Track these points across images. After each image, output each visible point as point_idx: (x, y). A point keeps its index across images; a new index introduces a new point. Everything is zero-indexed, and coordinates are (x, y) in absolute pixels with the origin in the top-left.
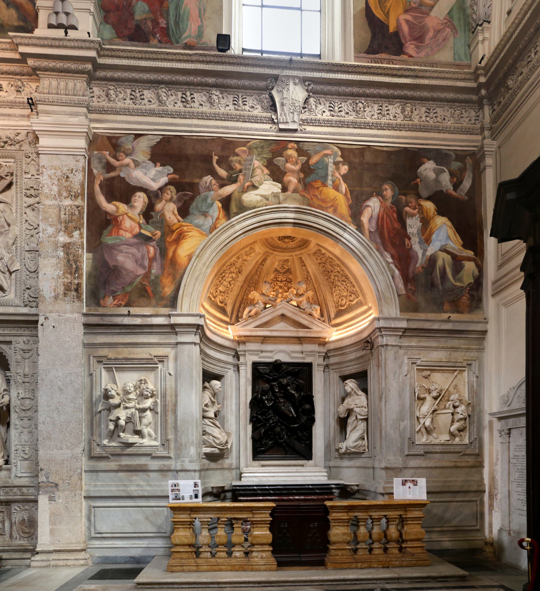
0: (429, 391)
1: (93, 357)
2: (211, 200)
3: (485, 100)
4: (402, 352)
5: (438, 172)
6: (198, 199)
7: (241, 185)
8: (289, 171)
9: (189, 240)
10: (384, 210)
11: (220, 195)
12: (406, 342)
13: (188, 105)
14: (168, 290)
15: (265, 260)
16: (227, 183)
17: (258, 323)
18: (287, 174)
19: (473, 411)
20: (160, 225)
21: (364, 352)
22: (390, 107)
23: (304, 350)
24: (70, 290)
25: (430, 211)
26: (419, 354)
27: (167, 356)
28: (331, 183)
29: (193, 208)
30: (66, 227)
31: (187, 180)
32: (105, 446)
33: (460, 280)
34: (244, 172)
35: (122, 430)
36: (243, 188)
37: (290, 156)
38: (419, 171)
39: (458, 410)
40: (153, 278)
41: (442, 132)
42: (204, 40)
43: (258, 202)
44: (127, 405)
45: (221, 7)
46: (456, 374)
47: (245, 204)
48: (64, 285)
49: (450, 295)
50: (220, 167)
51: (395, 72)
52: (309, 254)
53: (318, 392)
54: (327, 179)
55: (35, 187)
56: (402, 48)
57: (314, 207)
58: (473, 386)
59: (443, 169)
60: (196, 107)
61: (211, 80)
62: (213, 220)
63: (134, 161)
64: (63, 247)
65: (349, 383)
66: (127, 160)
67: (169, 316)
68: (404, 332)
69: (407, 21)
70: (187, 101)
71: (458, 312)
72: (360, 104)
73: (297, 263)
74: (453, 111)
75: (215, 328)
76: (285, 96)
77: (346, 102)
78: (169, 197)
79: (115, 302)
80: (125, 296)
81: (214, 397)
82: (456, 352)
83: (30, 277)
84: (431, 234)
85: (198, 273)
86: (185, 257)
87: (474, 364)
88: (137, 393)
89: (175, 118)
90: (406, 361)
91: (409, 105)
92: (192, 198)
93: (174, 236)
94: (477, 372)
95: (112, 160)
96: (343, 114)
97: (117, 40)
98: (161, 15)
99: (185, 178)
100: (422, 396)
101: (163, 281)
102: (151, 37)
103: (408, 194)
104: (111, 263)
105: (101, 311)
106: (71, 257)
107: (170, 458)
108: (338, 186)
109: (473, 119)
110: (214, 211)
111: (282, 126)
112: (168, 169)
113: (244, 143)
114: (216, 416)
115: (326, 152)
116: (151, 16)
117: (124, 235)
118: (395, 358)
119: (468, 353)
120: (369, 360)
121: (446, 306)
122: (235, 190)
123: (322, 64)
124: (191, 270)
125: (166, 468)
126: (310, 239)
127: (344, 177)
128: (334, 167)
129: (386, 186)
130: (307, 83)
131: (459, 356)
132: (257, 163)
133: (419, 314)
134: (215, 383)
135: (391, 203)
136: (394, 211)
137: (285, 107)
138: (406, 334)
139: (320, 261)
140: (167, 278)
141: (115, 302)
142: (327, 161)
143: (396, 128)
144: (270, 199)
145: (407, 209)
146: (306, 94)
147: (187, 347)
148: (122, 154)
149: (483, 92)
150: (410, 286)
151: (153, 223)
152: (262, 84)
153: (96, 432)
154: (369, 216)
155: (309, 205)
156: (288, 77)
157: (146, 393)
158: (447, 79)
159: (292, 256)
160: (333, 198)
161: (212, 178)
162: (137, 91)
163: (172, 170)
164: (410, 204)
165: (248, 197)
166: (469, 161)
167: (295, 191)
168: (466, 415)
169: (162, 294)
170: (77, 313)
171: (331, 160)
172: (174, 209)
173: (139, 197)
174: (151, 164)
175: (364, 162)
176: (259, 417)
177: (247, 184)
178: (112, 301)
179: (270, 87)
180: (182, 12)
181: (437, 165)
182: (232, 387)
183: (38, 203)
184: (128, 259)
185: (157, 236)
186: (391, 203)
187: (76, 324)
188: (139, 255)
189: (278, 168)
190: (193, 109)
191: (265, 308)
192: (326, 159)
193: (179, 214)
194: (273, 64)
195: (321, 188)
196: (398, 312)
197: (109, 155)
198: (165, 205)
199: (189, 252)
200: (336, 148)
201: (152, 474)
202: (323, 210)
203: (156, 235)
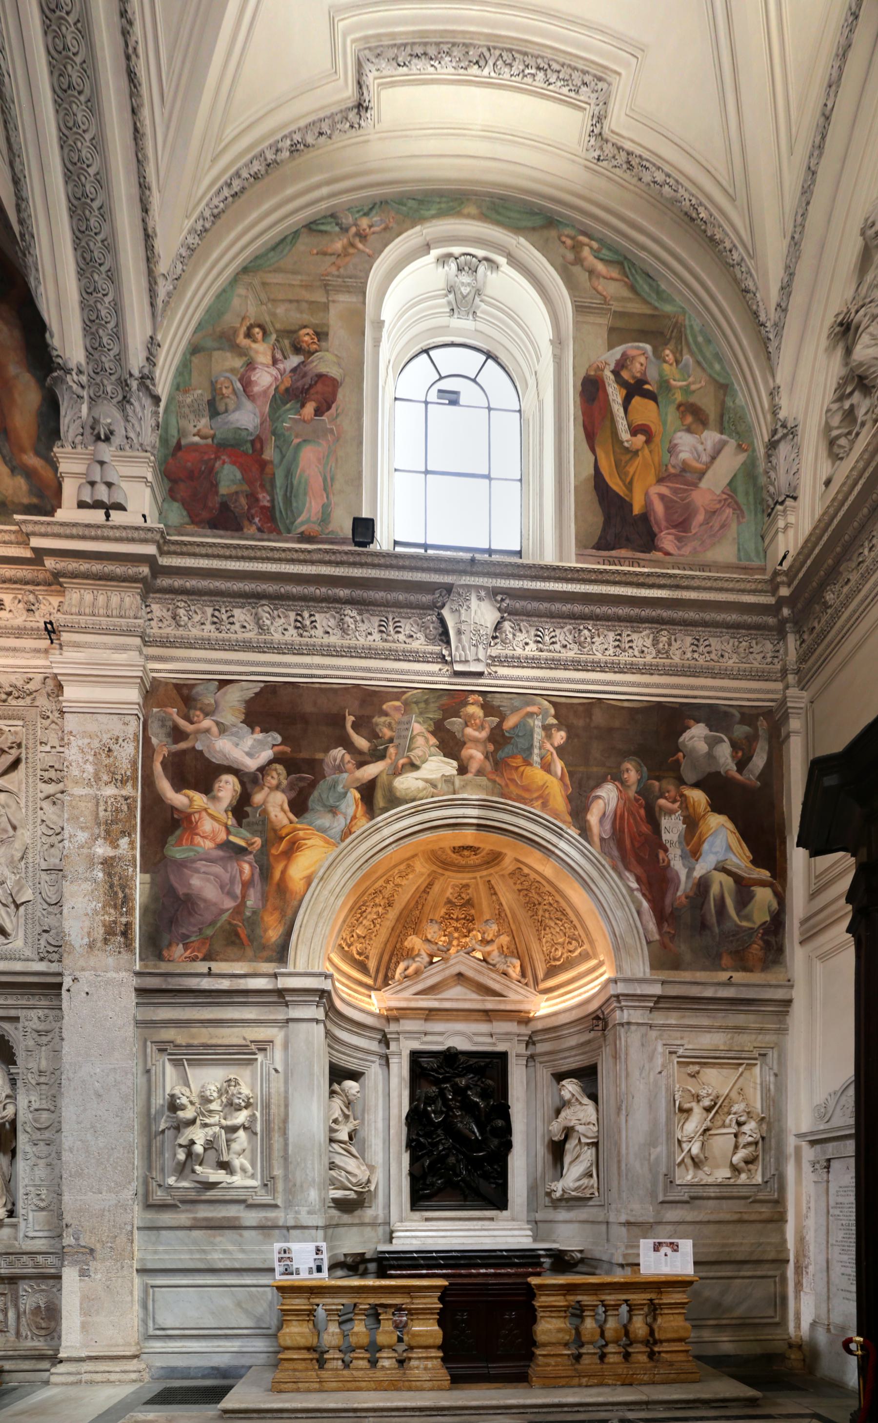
0: (698, 1098)
3: (788, 625)
4: (653, 1034)
5: (713, 743)
6: (322, 786)
9: (307, 852)
11: (358, 779)
12: (659, 1018)
13: (305, 634)
14: (273, 934)
15: (430, 885)
16: (369, 759)
17: (420, 987)
19: (769, 1130)
21: (592, 1034)
22: (634, 636)
23: (494, 1031)
24: (114, 934)
25: (699, 805)
26: (682, 1038)
28: (538, 760)
30: (108, 832)
31: (304, 755)
32: (170, 1187)
33: (748, 918)
34: (396, 741)
36: (396, 767)
37: (472, 716)
38: (681, 740)
39: (746, 1128)
42: (331, 527)
43: (419, 790)
44: (207, 1121)
45: (360, 473)
46: (741, 1070)
47: (398, 794)
48: (104, 925)
49: (732, 942)
51: (642, 580)
52: (503, 875)
53: (518, 1099)
54: (531, 754)
55: (56, 767)
56: (653, 541)
57: (510, 799)
60: (318, 637)
61: (343, 593)
63: (218, 723)
64: (102, 863)
66: (207, 723)
67: (275, 976)
68: (656, 1003)
69: (662, 497)
70: (304, 627)
71: (745, 969)
72: (586, 632)
73: (483, 889)
74: (736, 643)
75: (350, 995)
76: (463, 619)
77: (562, 628)
78: (274, 782)
79: (187, 954)
80: (204, 943)
81: (348, 1108)
83: (49, 913)
85: (322, 905)
87: (770, 1053)
89: (284, 653)
90: (660, 1049)
91: (664, 633)
92: (313, 785)
93: (283, 845)
94: (775, 1067)
95: (182, 723)
96: (557, 647)
97: (190, 528)
98: (262, 486)
100: (686, 1106)
101: (266, 919)
102: (246, 523)
103: (664, 777)
104: (181, 891)
105: (164, 967)
106: (116, 880)
107: (276, 1206)
108: (550, 765)
109: (769, 655)
110: (348, 806)
111: (458, 667)
114: (351, 1138)
115: (530, 709)
116: (245, 487)
118: (643, 1045)
119: (760, 1037)
120: (600, 1047)
121: (726, 960)
122: (382, 772)
123: (523, 566)
125: (269, 1224)
126: (504, 851)
127: (560, 750)
128: (543, 734)
129: (628, 765)
130: (499, 598)
131: (747, 1041)
132: (417, 727)
134: (350, 1085)
136: (641, 806)
137: (463, 636)
139: (520, 887)
140: (272, 914)
141: (187, 954)
144: (439, 786)
145: (662, 801)
146: (498, 615)
147: (304, 1026)
148: (198, 713)
149: (786, 612)
150: (666, 928)
151: (249, 824)
152: (426, 598)
153: (157, 1165)
154: (600, 814)
155: (503, 795)
156: (468, 587)
157: (237, 1101)
158: (727, 590)
159: (475, 878)
160: (541, 783)
162: (223, 610)
163: (279, 739)
166: (762, 724)
167: (480, 773)
168: (757, 1136)
169: (263, 941)
170: (126, 970)
171: (538, 723)
174: (245, 728)
175: (593, 725)
176: (422, 1140)
177: (401, 762)
179: (439, 604)
180: (295, 482)
181: (711, 730)
182: (377, 1092)
183: (62, 792)
184: (208, 884)
187: (123, 989)
188: (226, 877)
189: (452, 734)
190: (314, 639)
191: (431, 963)
192: (530, 721)
193: (292, 810)
194: (443, 566)
195: (522, 769)
196: (648, 970)
197: (178, 714)
198: (268, 795)
199: (307, 873)
200: (546, 703)
201: (247, 1234)
202: (525, 804)
203: (253, 844)
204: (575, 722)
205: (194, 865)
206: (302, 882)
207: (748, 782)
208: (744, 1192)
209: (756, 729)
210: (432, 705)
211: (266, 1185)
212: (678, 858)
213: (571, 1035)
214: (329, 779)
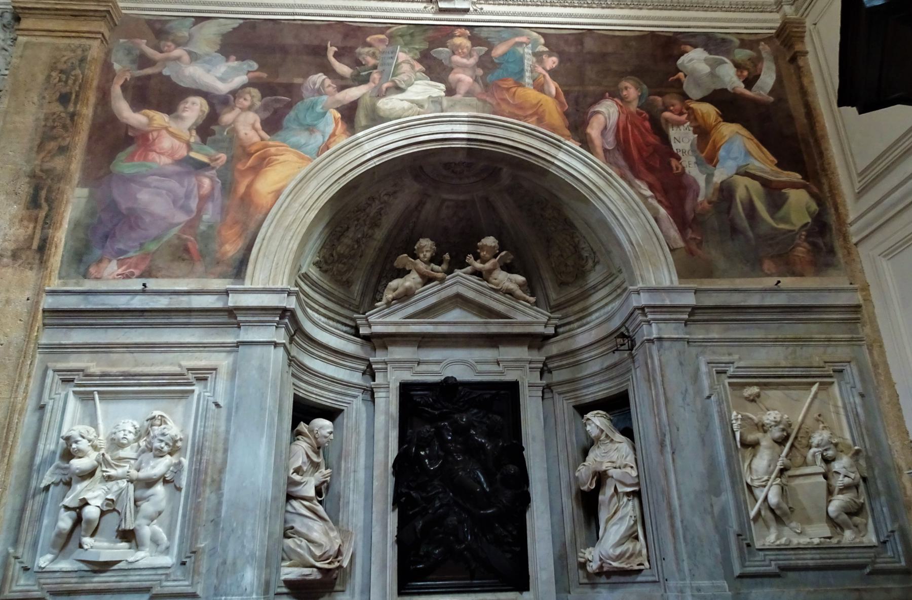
0: (762, 428)
1: (55, 371)
2: (322, 108)
4: (694, 350)
5: (714, 65)
6: (300, 106)
8: (458, 66)
9: (278, 168)
10: (627, 117)
11: (338, 101)
12: (698, 333)
14: (231, 249)
17: (411, 310)
18: (455, 71)
19: (870, 467)
23: (500, 358)
25: (709, 115)
27: (215, 369)
28: (531, 81)
31: (282, 79)
32: (42, 571)
34: (380, 68)
35: (91, 532)
36: (380, 90)
37: (459, 46)
38: (679, 62)
39: (837, 466)
40: (202, 227)
41: (710, 9)
43: (404, 109)
44: (112, 472)
46: (815, 388)
47: (382, 114)
53: (534, 439)
58: (857, 415)
59: (722, 59)
62: (324, 136)
63: (190, 53)
65: (593, 419)
66: (178, 52)
71: (794, 274)
78: (247, 104)
81: (317, 453)
82: (804, 348)
84: (715, 150)
85: (290, 219)
86: (269, 193)
87: (848, 368)
88: (139, 446)
90: (704, 368)
92: (290, 106)
93: (250, 162)
94: (859, 385)
95: (151, 52)
99: (277, 77)
100: (751, 437)
101: (223, 233)
104: (124, 205)
105: (88, 285)
108: (543, 85)
110: (327, 124)
113: (383, 29)
114: (319, 492)
115: (517, 39)
117: (158, 160)
118: (681, 364)
119: (830, 350)
120: (629, 371)
121: (768, 265)
122: (364, 95)
124: (276, 214)
127: (553, 73)
128: (534, 59)
129: (625, 83)
131: (815, 355)
133: (718, 280)
135: (638, 107)
138: (696, 318)
140: (231, 228)
141: (120, 271)
142: (522, 52)
143: (632, 6)
144: (426, 106)
145: (667, 114)
147: (258, 350)
148: (169, 44)
150: (690, 234)
151: (214, 142)
153: (26, 537)
154: (602, 127)
160: (535, 102)
161: (324, 77)
164: (672, 108)
165: (387, 104)
166: (765, 48)
167: (469, 93)
168: (855, 476)
169: (218, 255)
171: (527, 51)
173: (193, 103)
174: (220, 57)
175: (585, 51)
176: (413, 494)
177: (385, 85)
178: (116, 268)
181: (710, 53)
182: (358, 434)
185: (219, 161)
186: (638, 107)
188: (181, 191)
189: (440, 63)
192: (520, 50)
193: (263, 129)
195: (514, 90)
196: (675, 278)
197: (147, 44)
198: (239, 115)
200: (535, 34)
204: (567, 49)
205: (145, 180)
206: (270, 196)
207: (759, 97)
208: (856, 558)
209: (759, 52)
211: (184, 563)
212: (693, 165)
213: (592, 359)
214: (308, 101)
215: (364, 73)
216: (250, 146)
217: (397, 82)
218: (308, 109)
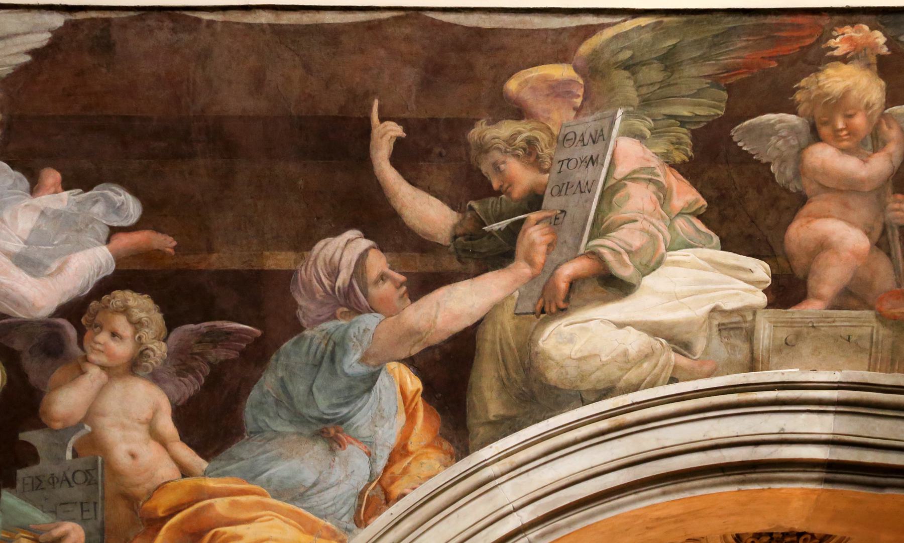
2: (363, 360)
7: (533, 278)
11: (413, 333)
16: (456, 266)
20: (77, 493)
29: (260, 404)
34: (551, 203)
36: (548, 287)
43: (627, 361)
47: (552, 375)
50: (412, 182)
78: (123, 350)
99: (210, 250)
110: (380, 416)
112: (110, 203)
122: (497, 306)
144: (700, 346)
151: (38, 484)
161: (365, 243)
163: (133, 208)
165: (571, 341)
172: (155, 412)
177: (568, 270)
193: (185, 436)
198: (102, 390)
210: (690, 71)
215: (496, 226)
216: (151, 494)
217: (608, 256)
218: (320, 364)
